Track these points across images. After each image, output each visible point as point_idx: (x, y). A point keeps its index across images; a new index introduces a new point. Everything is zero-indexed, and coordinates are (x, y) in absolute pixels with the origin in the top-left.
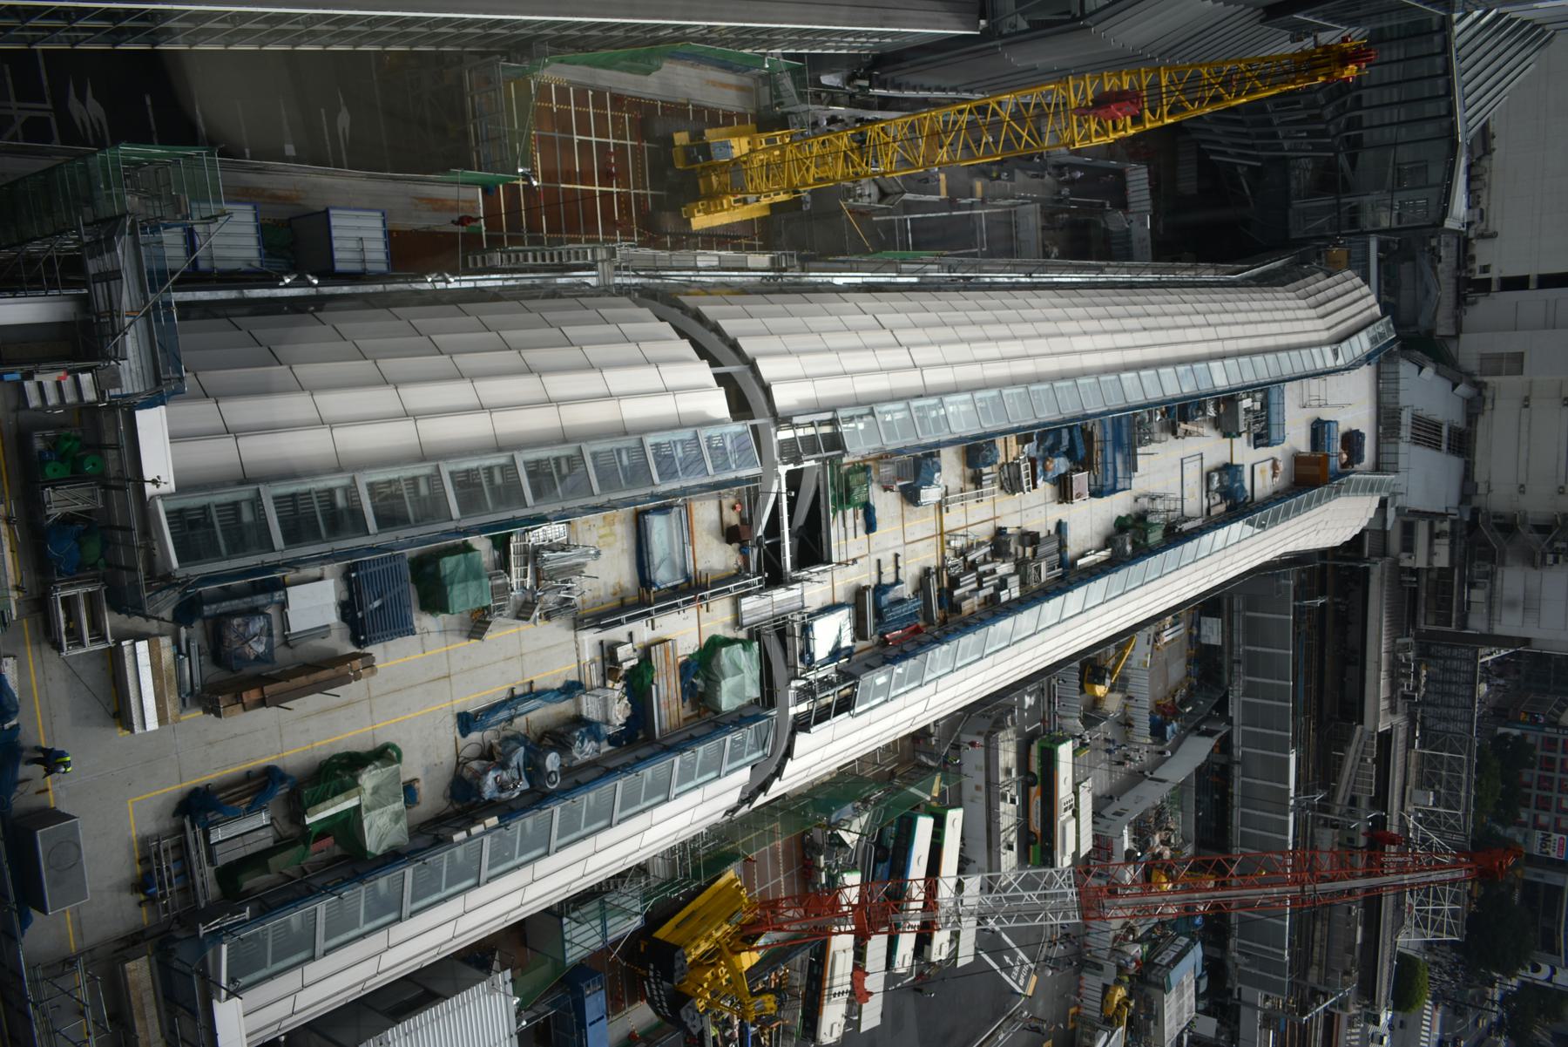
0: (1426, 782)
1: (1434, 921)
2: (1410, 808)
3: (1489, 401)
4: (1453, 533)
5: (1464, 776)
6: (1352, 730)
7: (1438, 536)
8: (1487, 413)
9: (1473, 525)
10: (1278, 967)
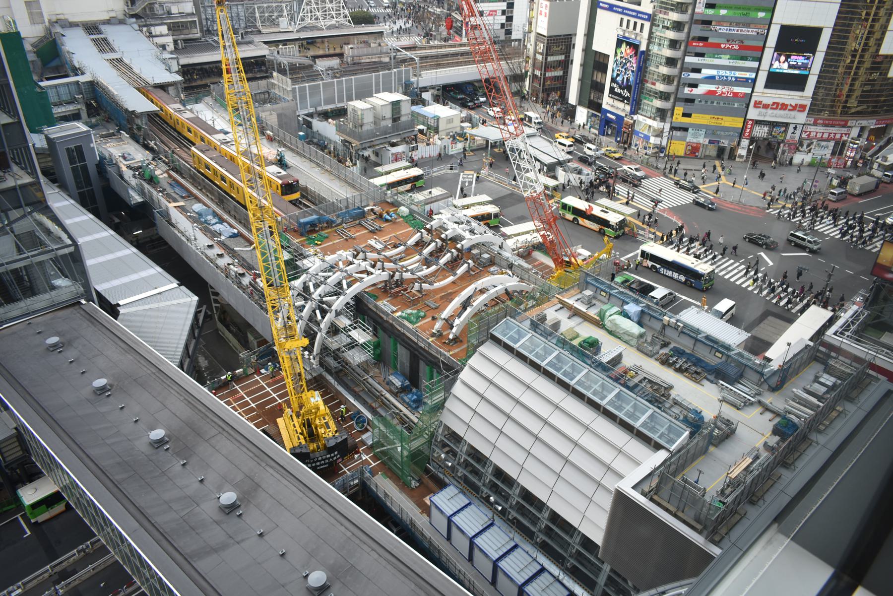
0: (273, 22)
2: (291, 29)
3: (59, 17)
4: (145, 26)
5: (265, 5)
6: (269, 61)
8: (66, 17)
9: (136, 16)
10: (400, 73)
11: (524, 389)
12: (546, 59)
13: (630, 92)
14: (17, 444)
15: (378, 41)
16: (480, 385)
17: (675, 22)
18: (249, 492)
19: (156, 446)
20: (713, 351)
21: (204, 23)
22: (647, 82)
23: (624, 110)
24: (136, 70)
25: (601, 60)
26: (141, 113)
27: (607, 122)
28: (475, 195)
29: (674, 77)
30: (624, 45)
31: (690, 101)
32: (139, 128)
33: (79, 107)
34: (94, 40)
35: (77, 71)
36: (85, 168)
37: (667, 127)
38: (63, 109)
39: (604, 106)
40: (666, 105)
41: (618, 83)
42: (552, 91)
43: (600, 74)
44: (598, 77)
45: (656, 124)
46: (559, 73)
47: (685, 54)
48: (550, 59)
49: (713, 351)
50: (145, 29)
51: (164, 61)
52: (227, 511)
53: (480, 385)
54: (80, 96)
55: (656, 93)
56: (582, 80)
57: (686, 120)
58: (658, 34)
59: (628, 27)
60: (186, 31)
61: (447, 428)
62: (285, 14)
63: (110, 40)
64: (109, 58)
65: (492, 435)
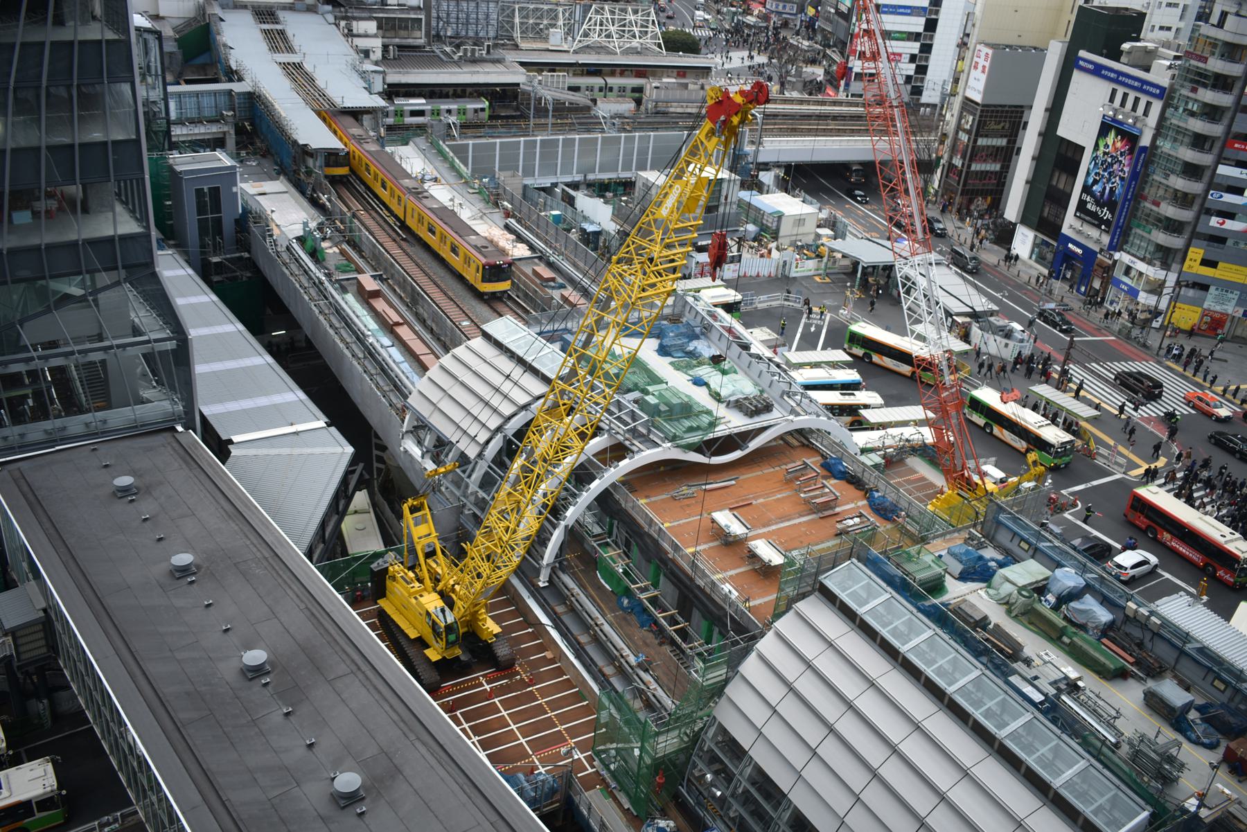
0: (540, 35)
1: (642, 26)
2: (565, 47)
4: (343, 18)
5: (532, 7)
7: (350, 30)
11: (865, 686)
12: (975, 141)
13: (1112, 213)
14: (41, 635)
15: (701, 81)
16: (790, 668)
17: (1206, 105)
18: (383, 778)
19: (250, 675)
20: (1210, 678)
21: (434, 23)
22: (1145, 199)
23: (1098, 241)
24: (320, 83)
25: (1070, 154)
26: (317, 150)
27: (1068, 257)
28: (824, 348)
29: (1195, 196)
30: (1112, 134)
31: (1218, 239)
32: (309, 173)
33: (226, 129)
34: (265, 32)
35: (233, 75)
36: (218, 222)
37: (1172, 278)
38: (202, 130)
39: (1065, 230)
40: (1176, 242)
41: (1092, 194)
42: (976, 192)
43: (1064, 177)
44: (1060, 182)
45: (1153, 272)
46: (996, 167)
47: (1220, 160)
48: (982, 142)
49: (1210, 678)
50: (343, 23)
51: (363, 75)
52: (342, 803)
53: (790, 668)
54: (231, 113)
55: (1159, 220)
56: (1032, 183)
57: (1208, 271)
58: (1174, 121)
59: (1123, 104)
60: (402, 33)
61: (723, 730)
62: (561, 22)
63: (289, 33)
64: (279, 60)
65: (797, 757)
